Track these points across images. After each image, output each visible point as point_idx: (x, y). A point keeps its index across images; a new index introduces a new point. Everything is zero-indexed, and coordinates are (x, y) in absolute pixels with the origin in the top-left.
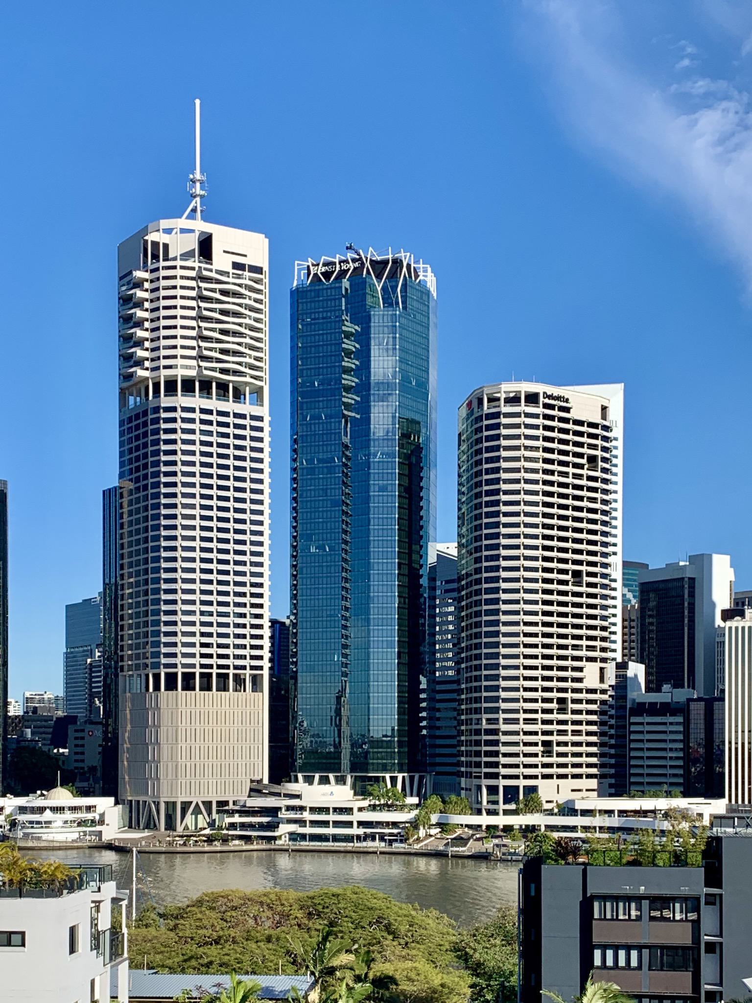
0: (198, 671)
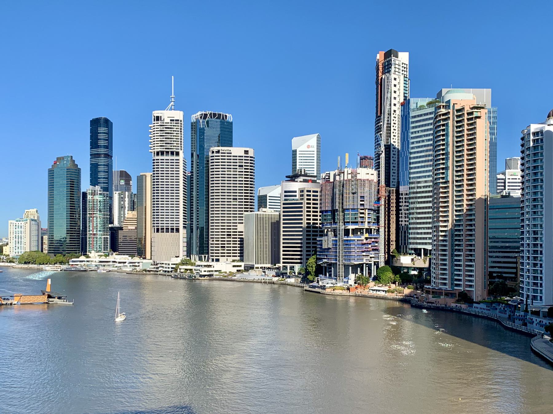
0: (160, 227)
